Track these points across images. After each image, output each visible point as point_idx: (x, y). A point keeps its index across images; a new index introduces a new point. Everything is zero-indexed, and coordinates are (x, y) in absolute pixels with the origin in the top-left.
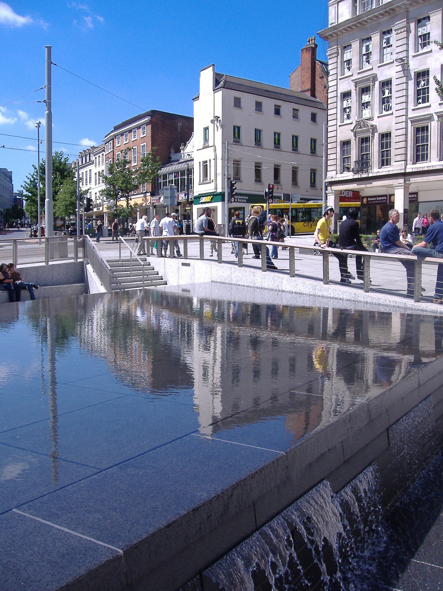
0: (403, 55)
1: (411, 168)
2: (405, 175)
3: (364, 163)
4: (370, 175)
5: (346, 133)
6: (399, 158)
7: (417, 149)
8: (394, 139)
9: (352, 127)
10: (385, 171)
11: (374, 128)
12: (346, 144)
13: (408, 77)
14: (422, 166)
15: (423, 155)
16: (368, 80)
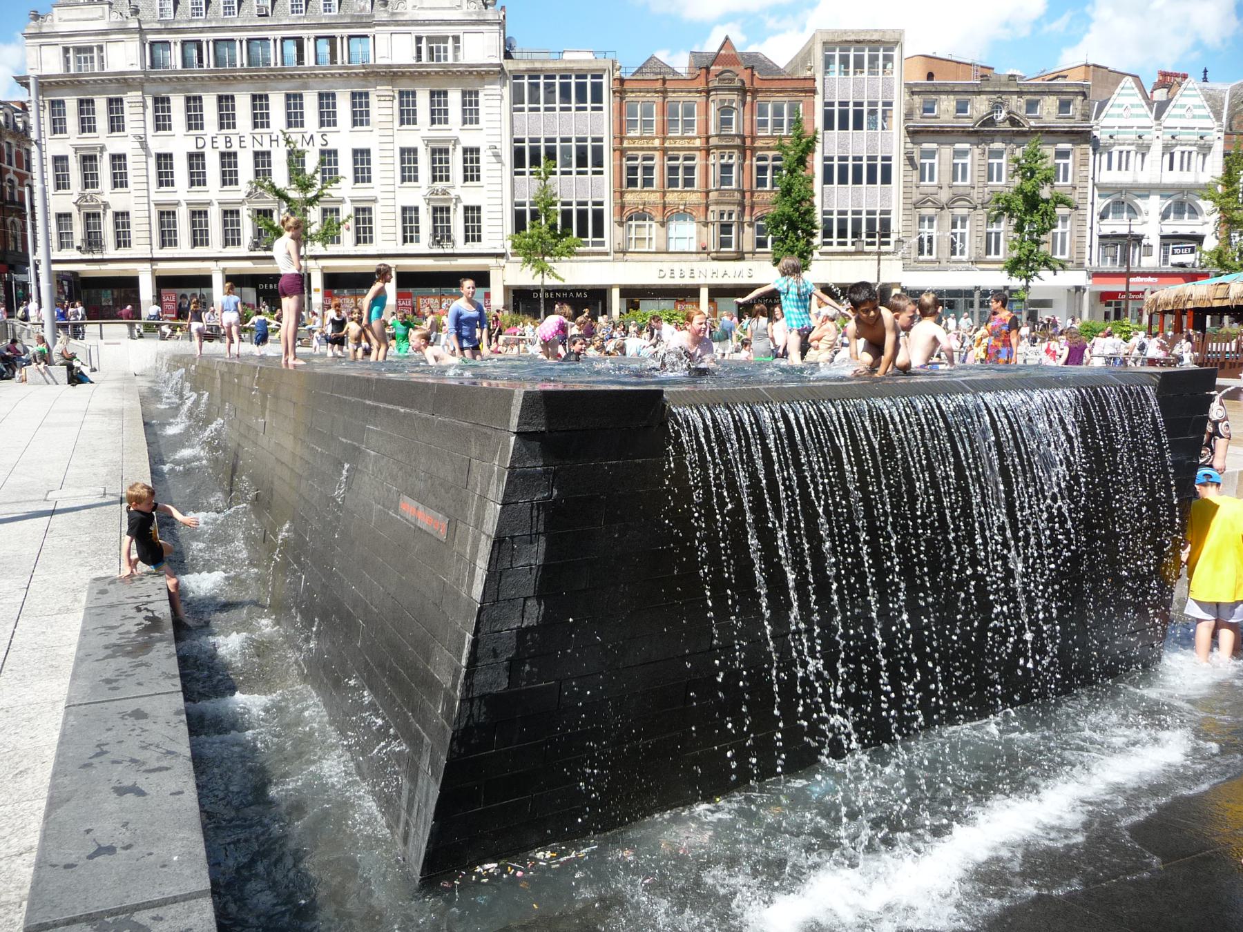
0: (141, 132)
1: (158, 253)
2: (152, 260)
3: (93, 241)
4: (106, 257)
5: (63, 202)
6: (142, 241)
7: (163, 233)
8: (133, 220)
9: (75, 198)
10: (123, 253)
11: (106, 205)
12: (63, 217)
13: (148, 155)
14: (168, 252)
15: (170, 241)
16: (95, 148)
